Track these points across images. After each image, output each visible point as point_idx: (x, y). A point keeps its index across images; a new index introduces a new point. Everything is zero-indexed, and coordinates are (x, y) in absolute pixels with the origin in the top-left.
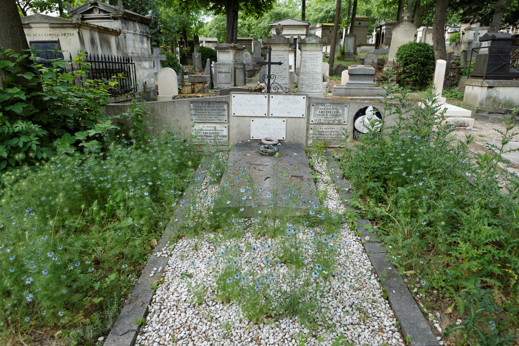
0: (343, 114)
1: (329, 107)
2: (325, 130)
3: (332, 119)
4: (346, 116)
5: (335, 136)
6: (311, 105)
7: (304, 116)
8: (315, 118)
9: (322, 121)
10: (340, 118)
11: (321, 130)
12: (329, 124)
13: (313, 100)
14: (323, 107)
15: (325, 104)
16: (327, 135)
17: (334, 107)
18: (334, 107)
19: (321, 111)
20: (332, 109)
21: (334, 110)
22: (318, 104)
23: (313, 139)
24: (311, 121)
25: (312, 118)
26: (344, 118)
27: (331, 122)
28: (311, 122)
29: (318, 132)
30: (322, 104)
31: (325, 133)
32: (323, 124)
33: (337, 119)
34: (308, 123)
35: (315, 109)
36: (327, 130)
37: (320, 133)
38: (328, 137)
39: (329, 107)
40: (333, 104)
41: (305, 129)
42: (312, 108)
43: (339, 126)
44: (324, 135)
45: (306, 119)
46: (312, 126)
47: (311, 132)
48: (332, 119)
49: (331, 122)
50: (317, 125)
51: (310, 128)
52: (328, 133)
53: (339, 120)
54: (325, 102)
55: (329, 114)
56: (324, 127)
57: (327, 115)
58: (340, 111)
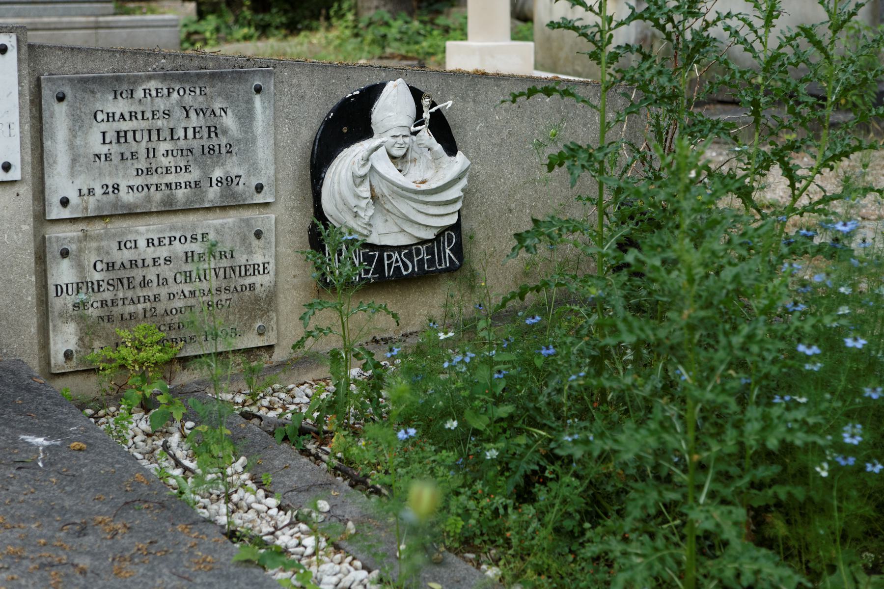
0: (249, 140)
1: (159, 99)
2: (150, 253)
3: (183, 177)
4: (263, 151)
5: (214, 283)
6: (47, 93)
7: (15, 174)
8: (83, 182)
9: (127, 197)
10: (233, 167)
11: (127, 255)
12: (169, 210)
13: (53, 63)
14: (121, 106)
15: (136, 81)
16: (162, 282)
17: (188, 100)
18: (188, 100)
19: (111, 128)
20: (179, 113)
21: (195, 120)
22: (89, 84)
23: (81, 319)
24: (54, 199)
25: (62, 182)
26: (254, 168)
27: (181, 194)
28: (56, 212)
29: (110, 266)
30: (119, 85)
31: (151, 275)
32: (131, 214)
33: (217, 173)
34: (41, 218)
35: (77, 125)
36: (163, 252)
37: (122, 275)
38: (173, 296)
39: (161, 104)
40: (184, 78)
41: (28, 259)
42: (59, 117)
43: (231, 219)
44: (145, 283)
45: (26, 191)
46: (67, 234)
47: (63, 273)
48: (183, 177)
49: (181, 194)
50: (97, 228)
51: (54, 249)
52: (167, 271)
53: (228, 182)
54: (128, 68)
55: (163, 147)
56: (142, 230)
57: (151, 153)
58: (229, 121)
